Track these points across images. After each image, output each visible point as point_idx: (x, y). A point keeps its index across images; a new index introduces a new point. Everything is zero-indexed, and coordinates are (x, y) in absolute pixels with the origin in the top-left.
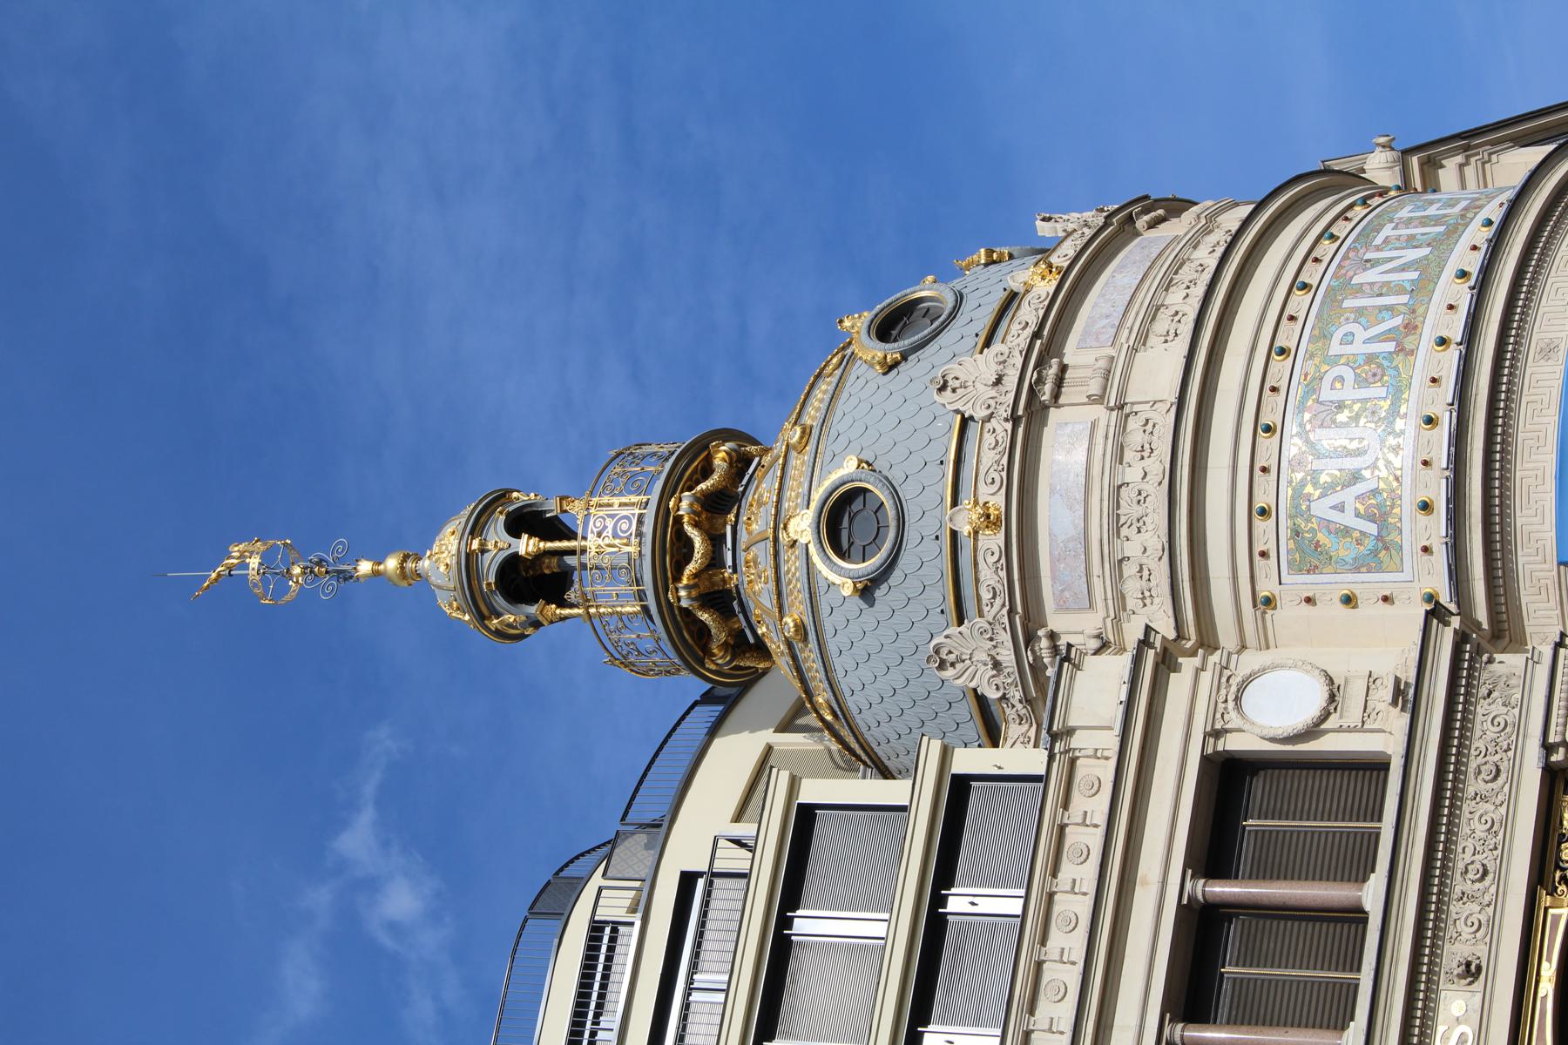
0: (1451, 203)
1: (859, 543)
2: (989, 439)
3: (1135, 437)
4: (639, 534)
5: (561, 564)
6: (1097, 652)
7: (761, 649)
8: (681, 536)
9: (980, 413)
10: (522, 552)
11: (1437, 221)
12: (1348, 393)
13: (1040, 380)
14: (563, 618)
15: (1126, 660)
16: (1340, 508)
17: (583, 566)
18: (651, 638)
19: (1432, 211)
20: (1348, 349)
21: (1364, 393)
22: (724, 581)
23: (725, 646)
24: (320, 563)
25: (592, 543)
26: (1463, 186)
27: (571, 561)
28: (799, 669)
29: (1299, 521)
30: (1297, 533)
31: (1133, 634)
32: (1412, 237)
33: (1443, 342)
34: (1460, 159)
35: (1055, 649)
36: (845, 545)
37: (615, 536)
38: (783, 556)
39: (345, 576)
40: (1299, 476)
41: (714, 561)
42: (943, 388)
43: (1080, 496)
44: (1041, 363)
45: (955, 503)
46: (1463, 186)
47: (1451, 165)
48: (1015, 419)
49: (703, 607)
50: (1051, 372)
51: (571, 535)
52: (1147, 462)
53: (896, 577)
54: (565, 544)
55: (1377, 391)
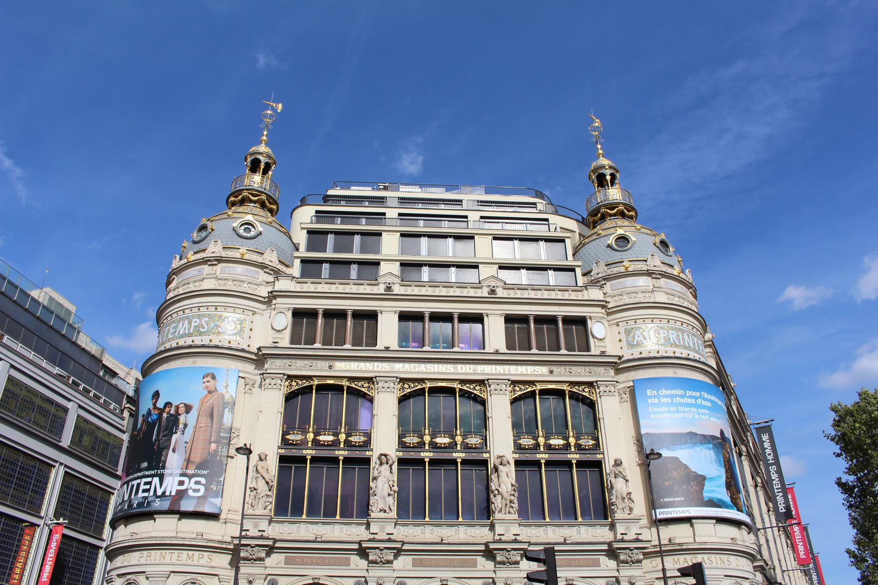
0: (703, 351)
1: (618, 243)
3: (647, 295)
4: (614, 200)
5: (606, 185)
6: (603, 293)
7: (594, 227)
8: (615, 208)
10: (607, 177)
11: (699, 348)
12: (662, 336)
14: (595, 187)
15: (602, 299)
16: (638, 337)
17: (606, 190)
18: (593, 205)
19: (701, 347)
20: (670, 334)
21: (662, 338)
22: (607, 218)
23: (594, 220)
24: (598, 137)
25: (611, 191)
26: (707, 353)
27: (607, 187)
28: (592, 235)
29: (635, 329)
30: (632, 329)
31: (608, 299)
32: (695, 344)
33: (674, 353)
34: (712, 351)
35: (603, 285)
36: (618, 240)
37: (613, 195)
38: (613, 229)
39: (597, 143)
40: (644, 328)
41: (611, 215)
43: (634, 285)
45: (629, 261)
46: (707, 353)
47: (711, 350)
49: (601, 214)
51: (612, 186)
53: (613, 251)
54: (610, 185)
55: (663, 341)
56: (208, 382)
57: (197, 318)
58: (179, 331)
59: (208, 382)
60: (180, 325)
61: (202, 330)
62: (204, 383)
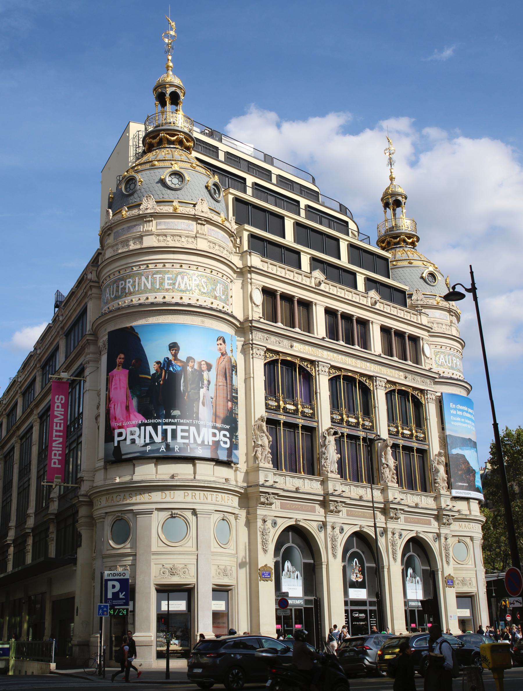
2: (191, 210)
9: (196, 208)
13: (202, 221)
42: (202, 200)
44: (205, 221)
48: (195, 215)
50: (204, 223)
52: (185, 242)
56: (221, 344)
57: (197, 277)
58: (179, 284)
59: (221, 344)
60: (179, 278)
61: (202, 290)
62: (218, 345)
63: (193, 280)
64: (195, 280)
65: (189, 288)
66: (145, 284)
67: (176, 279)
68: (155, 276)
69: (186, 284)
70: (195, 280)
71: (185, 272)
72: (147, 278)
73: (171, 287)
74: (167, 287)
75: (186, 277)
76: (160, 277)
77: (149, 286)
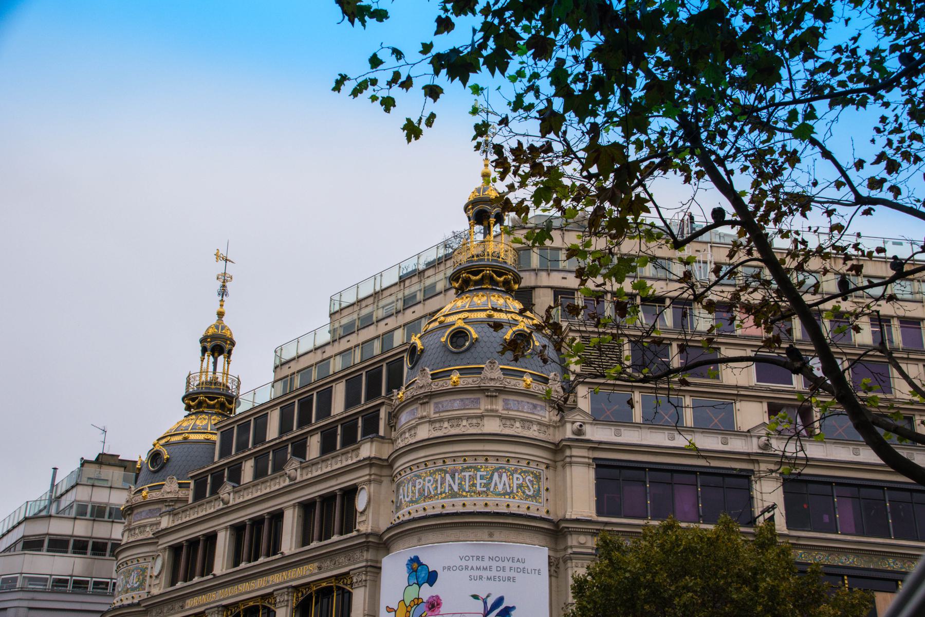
57: (520, 474)
58: (496, 484)
60: (496, 475)
61: (527, 492)
63: (515, 479)
64: (517, 478)
65: (509, 491)
66: (450, 485)
67: (491, 478)
68: (463, 474)
69: (505, 484)
70: (517, 478)
71: (504, 468)
72: (453, 477)
73: (485, 489)
74: (479, 489)
75: (504, 475)
76: (470, 476)
77: (456, 488)
